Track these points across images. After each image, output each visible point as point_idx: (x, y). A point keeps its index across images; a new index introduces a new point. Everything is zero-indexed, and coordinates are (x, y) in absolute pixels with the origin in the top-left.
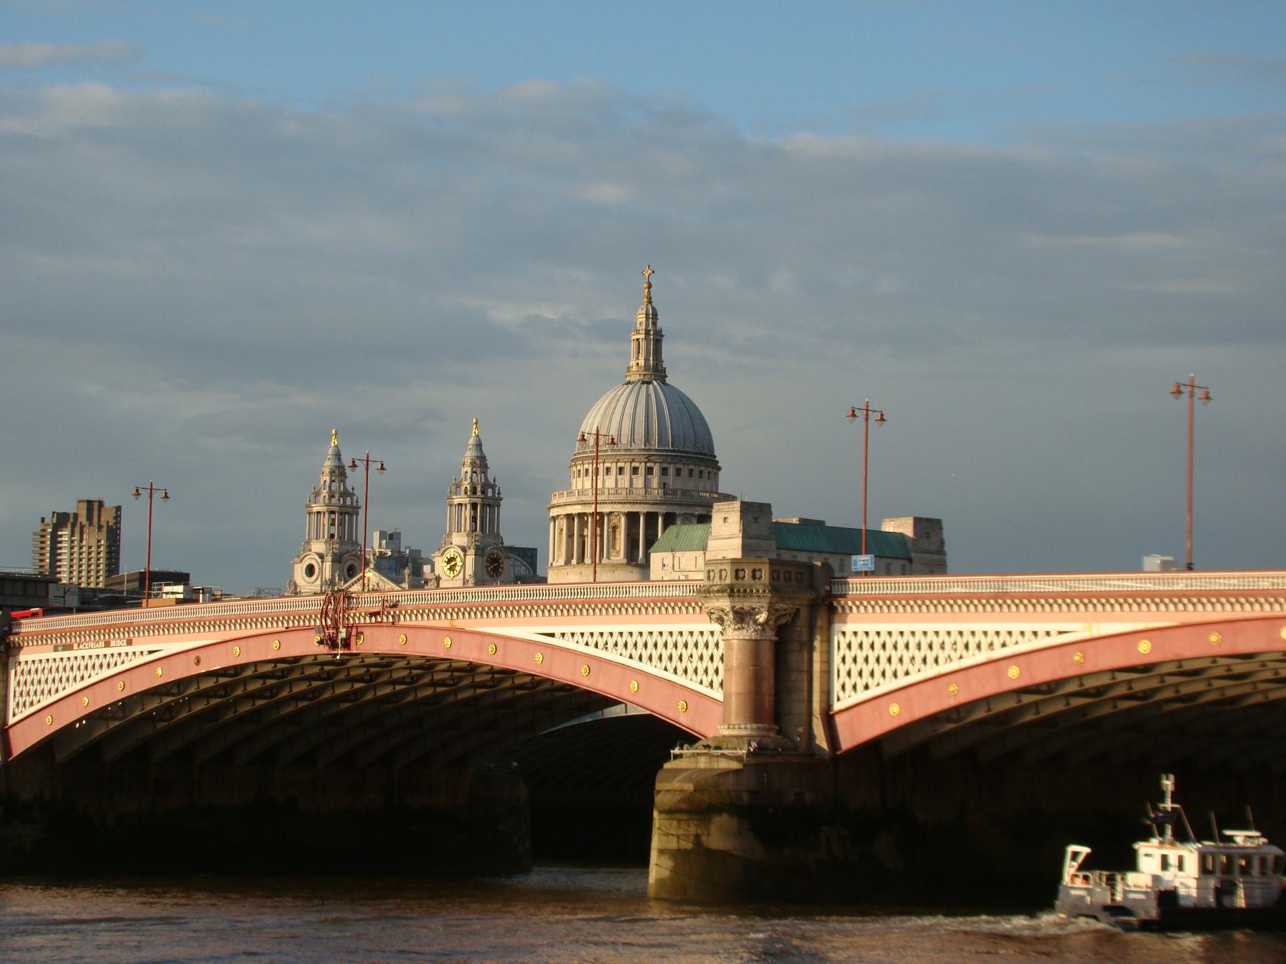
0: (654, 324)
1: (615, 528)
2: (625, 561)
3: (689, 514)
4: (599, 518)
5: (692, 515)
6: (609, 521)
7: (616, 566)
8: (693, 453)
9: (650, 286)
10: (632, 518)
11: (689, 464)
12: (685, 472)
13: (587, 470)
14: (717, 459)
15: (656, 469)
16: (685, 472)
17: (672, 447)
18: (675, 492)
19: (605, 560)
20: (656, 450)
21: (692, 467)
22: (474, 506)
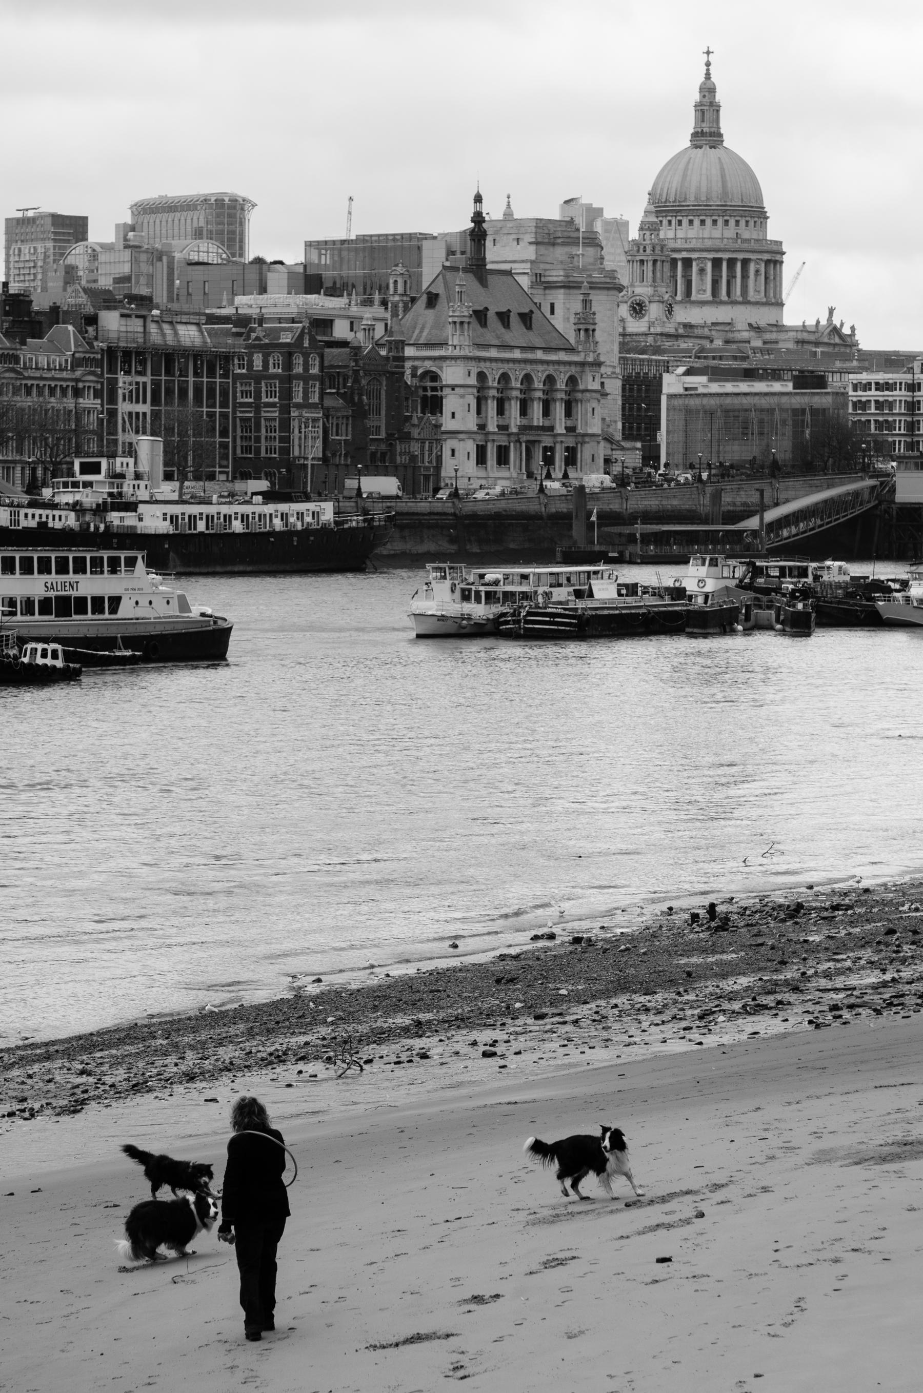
1: (702, 271)
2: (710, 298)
5: (761, 260)
6: (698, 265)
7: (703, 303)
9: (708, 64)
10: (717, 263)
12: (751, 224)
13: (670, 222)
15: (732, 222)
16: (751, 224)
19: (693, 298)
20: (731, 206)
21: (756, 219)
22: (655, 262)
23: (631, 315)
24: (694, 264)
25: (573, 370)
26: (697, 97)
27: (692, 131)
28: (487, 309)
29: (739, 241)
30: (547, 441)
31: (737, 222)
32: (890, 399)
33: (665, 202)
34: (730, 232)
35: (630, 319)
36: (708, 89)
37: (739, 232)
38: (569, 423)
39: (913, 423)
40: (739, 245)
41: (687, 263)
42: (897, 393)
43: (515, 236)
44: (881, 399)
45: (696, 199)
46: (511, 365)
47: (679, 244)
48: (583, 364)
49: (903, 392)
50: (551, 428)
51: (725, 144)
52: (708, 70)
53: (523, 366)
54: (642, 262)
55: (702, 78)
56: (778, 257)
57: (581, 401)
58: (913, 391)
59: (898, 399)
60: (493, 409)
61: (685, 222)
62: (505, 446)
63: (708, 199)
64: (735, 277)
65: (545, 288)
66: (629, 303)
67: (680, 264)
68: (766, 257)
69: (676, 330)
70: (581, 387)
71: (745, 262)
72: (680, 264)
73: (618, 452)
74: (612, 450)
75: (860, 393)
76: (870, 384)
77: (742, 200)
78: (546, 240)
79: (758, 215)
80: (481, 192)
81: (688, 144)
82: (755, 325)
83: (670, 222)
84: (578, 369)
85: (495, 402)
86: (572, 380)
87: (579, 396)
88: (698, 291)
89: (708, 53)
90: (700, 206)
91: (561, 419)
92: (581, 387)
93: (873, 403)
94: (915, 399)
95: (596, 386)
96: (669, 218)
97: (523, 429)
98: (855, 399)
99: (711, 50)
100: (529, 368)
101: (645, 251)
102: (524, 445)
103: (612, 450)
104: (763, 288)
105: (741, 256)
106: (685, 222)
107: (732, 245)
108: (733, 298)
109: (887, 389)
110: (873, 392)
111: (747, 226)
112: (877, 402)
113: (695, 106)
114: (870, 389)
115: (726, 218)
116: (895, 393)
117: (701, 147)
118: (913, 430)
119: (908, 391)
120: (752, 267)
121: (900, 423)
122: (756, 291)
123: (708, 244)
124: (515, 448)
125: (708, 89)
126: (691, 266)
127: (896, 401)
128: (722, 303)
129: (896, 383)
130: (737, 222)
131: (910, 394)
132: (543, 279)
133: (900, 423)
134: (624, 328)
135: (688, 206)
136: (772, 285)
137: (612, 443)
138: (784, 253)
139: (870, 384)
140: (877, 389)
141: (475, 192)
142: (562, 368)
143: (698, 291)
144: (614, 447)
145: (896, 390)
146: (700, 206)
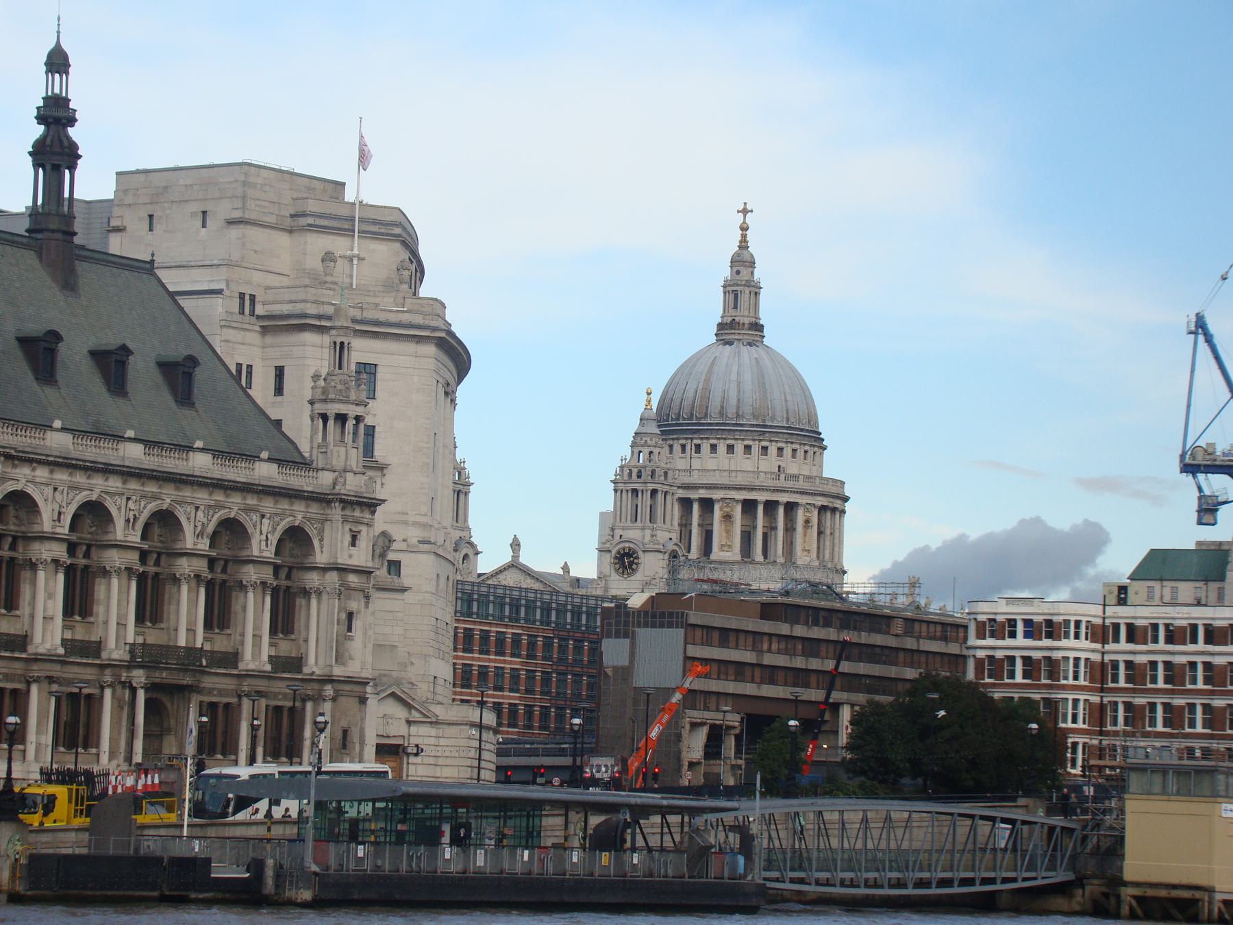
0: (752, 273)
1: (727, 517)
2: (738, 557)
3: (810, 504)
4: (707, 504)
6: (721, 509)
8: (808, 431)
9: (744, 228)
11: (804, 444)
12: (800, 454)
13: (683, 447)
14: (821, 436)
15: (773, 450)
16: (800, 454)
17: (787, 423)
18: (795, 477)
20: (771, 427)
21: (807, 448)
22: (654, 492)
23: (617, 570)
24: (717, 507)
26: (726, 272)
27: (720, 320)
28: (55, 336)
29: (782, 476)
30: (217, 684)
31: (780, 450)
32: (1057, 655)
33: (678, 419)
34: (770, 463)
35: (615, 576)
36: (742, 261)
37: (783, 465)
38: (286, 648)
39: (1102, 706)
40: (782, 483)
41: (707, 504)
42: (1071, 642)
43: (198, 207)
44: (1037, 655)
45: (721, 414)
46: (115, 483)
47: (695, 479)
48: (322, 499)
49: (1084, 643)
50: (232, 659)
51: (766, 341)
52: (744, 237)
53: (152, 488)
54: (635, 491)
55: (735, 248)
56: (837, 504)
57: (319, 593)
58: (1104, 641)
59: (1072, 655)
60: (50, 596)
61: (705, 447)
62: (89, 697)
64: (774, 528)
65: (265, 330)
66: (614, 552)
67: (696, 507)
68: (820, 501)
70: (321, 557)
71: (791, 507)
72: (696, 507)
73: (425, 730)
74: (409, 723)
75: (990, 642)
76: (1012, 623)
77: (788, 419)
78: (271, 219)
79: (814, 440)
80: (65, 46)
81: (714, 339)
83: (683, 447)
84: (315, 509)
85: (61, 577)
86: (296, 538)
87: (312, 580)
88: (722, 547)
90: (728, 424)
91: (257, 637)
92: (321, 558)
93: (1019, 664)
94: (1107, 658)
95: (361, 556)
96: (683, 442)
97: (145, 657)
98: (981, 654)
99: (749, 208)
100: (168, 497)
101: (639, 476)
102: (141, 696)
103: (409, 723)
104: (815, 546)
105: (784, 498)
106: (705, 447)
107: (769, 483)
108: (771, 558)
109: (1050, 635)
110: (1020, 640)
111: (794, 456)
112: (1027, 660)
113: (724, 287)
114: (1013, 635)
115: (763, 443)
116: (1064, 643)
117: (730, 343)
118: (1102, 723)
119: (1093, 641)
120: (800, 515)
121: (1075, 706)
122: (804, 550)
123: (740, 480)
124: (118, 704)
125: (742, 261)
126: (712, 511)
127: (1066, 659)
128: (753, 562)
129: (1067, 622)
130: (780, 450)
131: (1098, 646)
132: (260, 310)
133: (1075, 706)
134: (606, 589)
135: (710, 424)
136: (828, 543)
137: (409, 706)
138: (846, 499)
139: (1012, 623)
140: (1027, 635)
141: (52, 45)
142: (268, 505)
144: (416, 716)
145: (1067, 636)
146: (728, 424)
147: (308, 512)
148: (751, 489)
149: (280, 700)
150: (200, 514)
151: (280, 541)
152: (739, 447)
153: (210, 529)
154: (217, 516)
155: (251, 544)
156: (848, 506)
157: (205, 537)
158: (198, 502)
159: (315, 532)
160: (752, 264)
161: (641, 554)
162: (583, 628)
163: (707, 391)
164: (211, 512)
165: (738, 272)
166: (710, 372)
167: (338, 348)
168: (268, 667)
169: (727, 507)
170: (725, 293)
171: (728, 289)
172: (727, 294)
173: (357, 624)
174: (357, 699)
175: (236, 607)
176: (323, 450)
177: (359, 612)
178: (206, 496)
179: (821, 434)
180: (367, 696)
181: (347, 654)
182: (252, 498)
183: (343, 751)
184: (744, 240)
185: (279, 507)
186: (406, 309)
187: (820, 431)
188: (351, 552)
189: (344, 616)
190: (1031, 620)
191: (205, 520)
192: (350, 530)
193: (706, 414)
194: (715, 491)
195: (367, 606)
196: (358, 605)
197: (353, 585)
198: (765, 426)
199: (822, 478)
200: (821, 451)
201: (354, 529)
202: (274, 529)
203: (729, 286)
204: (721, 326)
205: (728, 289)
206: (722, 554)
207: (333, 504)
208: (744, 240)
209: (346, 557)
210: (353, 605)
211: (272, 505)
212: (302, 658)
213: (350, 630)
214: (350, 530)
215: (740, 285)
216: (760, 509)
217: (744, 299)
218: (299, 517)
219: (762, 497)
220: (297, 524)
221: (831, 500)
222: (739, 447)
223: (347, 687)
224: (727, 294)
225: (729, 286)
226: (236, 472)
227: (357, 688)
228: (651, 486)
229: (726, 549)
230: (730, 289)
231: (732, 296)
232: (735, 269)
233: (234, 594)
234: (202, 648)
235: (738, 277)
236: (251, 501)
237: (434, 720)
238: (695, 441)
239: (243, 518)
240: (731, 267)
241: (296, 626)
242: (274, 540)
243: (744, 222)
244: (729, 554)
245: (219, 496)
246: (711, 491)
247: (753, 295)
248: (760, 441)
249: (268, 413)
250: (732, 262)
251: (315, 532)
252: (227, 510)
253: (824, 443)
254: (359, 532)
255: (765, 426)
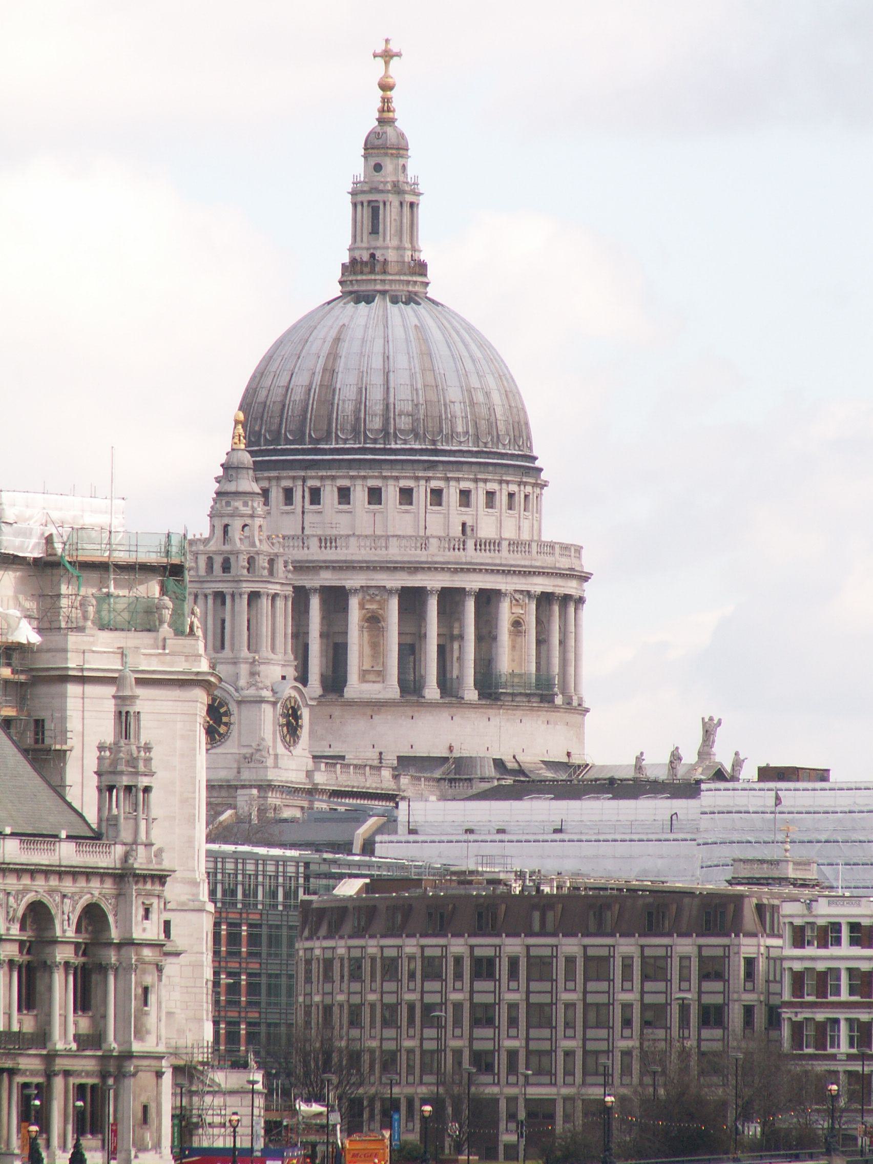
1: (374, 621)
3: (521, 592)
6: (362, 606)
7: (376, 706)
14: (537, 464)
15: (452, 495)
18: (493, 545)
21: (513, 488)
24: (354, 603)
25: (97, 891)
40: (470, 555)
52: (386, 101)
54: (220, 597)
56: (570, 587)
63: (385, 432)
64: (461, 637)
67: (315, 603)
68: (540, 585)
69: (309, 774)
72: (315, 603)
77: (477, 437)
81: (337, 291)
82: (511, 765)
88: (364, 676)
89: (387, 56)
96: (287, 483)
98: (798, 966)
105: (474, 583)
110: (845, 949)
113: (354, 193)
115: (434, 484)
117: (369, 299)
120: (505, 613)
123: (395, 552)
126: (345, 609)
139: (836, 927)
140: (854, 942)
143: (364, 676)
147: (103, 888)
148: (415, 568)
149: (82, 1077)
150: (11, 899)
151: (80, 918)
152: (391, 493)
153: (20, 913)
154: (25, 900)
155: (54, 925)
156: (589, 590)
157: (15, 921)
158: (9, 889)
159: (110, 907)
160: (399, 149)
161: (233, 707)
162: (239, 906)
163: (329, 388)
164: (20, 897)
165: (378, 168)
166: (333, 355)
167: (124, 718)
168: (74, 1046)
169: (372, 600)
170: (355, 205)
171: (360, 198)
172: (359, 208)
173: (152, 998)
174: (154, 1074)
175: (40, 987)
176: (112, 823)
177: (153, 986)
178: (15, 882)
179: (535, 458)
180: (164, 1070)
181: (144, 1029)
182: (54, 880)
183: (144, 1126)
184: (386, 107)
185: (78, 885)
186: (167, 651)
187: (535, 453)
188: (145, 926)
189: (140, 991)
190: (859, 924)
191: (15, 906)
192: (143, 903)
193: (329, 432)
194: (348, 574)
195: (160, 979)
196: (153, 979)
197: (147, 959)
198: (436, 452)
199: (541, 544)
200: (538, 490)
201: (147, 902)
202: (74, 908)
203: (363, 192)
204: (353, 268)
205: (360, 198)
206: (366, 687)
207: (126, 879)
208: (386, 107)
209: (140, 931)
210: (149, 980)
211: (71, 885)
212: (100, 1035)
213: (146, 1004)
214: (143, 903)
215: (382, 191)
216: (433, 605)
217: (390, 216)
218: (96, 893)
219: (434, 582)
220: (94, 901)
221: (560, 582)
222: (391, 493)
223: (146, 1062)
224: (359, 208)
225: (363, 192)
226: (40, 857)
227: (153, 1063)
228: (247, 588)
229: (371, 677)
230: (365, 198)
231: (367, 212)
232: (372, 162)
233: (38, 974)
234: (20, 1032)
235: (378, 177)
236: (54, 882)
237: (216, 1089)
238: (310, 483)
239: (46, 900)
240: (366, 157)
241: (93, 1002)
242: (74, 919)
243: (386, 76)
244: (378, 687)
245: (26, 880)
246: (342, 575)
247: (406, 209)
248: (428, 479)
249: (40, 779)
250: (366, 149)
251: (110, 907)
252: (33, 894)
253: (543, 474)
254: (151, 905)
255: (436, 452)
